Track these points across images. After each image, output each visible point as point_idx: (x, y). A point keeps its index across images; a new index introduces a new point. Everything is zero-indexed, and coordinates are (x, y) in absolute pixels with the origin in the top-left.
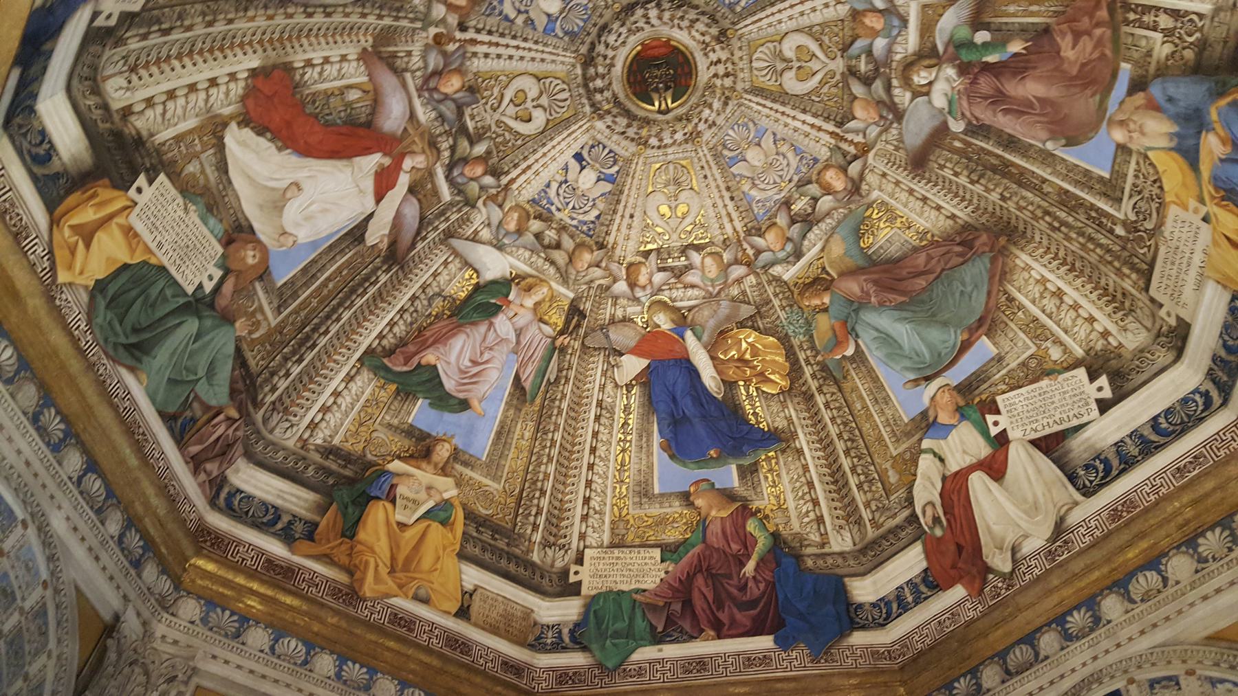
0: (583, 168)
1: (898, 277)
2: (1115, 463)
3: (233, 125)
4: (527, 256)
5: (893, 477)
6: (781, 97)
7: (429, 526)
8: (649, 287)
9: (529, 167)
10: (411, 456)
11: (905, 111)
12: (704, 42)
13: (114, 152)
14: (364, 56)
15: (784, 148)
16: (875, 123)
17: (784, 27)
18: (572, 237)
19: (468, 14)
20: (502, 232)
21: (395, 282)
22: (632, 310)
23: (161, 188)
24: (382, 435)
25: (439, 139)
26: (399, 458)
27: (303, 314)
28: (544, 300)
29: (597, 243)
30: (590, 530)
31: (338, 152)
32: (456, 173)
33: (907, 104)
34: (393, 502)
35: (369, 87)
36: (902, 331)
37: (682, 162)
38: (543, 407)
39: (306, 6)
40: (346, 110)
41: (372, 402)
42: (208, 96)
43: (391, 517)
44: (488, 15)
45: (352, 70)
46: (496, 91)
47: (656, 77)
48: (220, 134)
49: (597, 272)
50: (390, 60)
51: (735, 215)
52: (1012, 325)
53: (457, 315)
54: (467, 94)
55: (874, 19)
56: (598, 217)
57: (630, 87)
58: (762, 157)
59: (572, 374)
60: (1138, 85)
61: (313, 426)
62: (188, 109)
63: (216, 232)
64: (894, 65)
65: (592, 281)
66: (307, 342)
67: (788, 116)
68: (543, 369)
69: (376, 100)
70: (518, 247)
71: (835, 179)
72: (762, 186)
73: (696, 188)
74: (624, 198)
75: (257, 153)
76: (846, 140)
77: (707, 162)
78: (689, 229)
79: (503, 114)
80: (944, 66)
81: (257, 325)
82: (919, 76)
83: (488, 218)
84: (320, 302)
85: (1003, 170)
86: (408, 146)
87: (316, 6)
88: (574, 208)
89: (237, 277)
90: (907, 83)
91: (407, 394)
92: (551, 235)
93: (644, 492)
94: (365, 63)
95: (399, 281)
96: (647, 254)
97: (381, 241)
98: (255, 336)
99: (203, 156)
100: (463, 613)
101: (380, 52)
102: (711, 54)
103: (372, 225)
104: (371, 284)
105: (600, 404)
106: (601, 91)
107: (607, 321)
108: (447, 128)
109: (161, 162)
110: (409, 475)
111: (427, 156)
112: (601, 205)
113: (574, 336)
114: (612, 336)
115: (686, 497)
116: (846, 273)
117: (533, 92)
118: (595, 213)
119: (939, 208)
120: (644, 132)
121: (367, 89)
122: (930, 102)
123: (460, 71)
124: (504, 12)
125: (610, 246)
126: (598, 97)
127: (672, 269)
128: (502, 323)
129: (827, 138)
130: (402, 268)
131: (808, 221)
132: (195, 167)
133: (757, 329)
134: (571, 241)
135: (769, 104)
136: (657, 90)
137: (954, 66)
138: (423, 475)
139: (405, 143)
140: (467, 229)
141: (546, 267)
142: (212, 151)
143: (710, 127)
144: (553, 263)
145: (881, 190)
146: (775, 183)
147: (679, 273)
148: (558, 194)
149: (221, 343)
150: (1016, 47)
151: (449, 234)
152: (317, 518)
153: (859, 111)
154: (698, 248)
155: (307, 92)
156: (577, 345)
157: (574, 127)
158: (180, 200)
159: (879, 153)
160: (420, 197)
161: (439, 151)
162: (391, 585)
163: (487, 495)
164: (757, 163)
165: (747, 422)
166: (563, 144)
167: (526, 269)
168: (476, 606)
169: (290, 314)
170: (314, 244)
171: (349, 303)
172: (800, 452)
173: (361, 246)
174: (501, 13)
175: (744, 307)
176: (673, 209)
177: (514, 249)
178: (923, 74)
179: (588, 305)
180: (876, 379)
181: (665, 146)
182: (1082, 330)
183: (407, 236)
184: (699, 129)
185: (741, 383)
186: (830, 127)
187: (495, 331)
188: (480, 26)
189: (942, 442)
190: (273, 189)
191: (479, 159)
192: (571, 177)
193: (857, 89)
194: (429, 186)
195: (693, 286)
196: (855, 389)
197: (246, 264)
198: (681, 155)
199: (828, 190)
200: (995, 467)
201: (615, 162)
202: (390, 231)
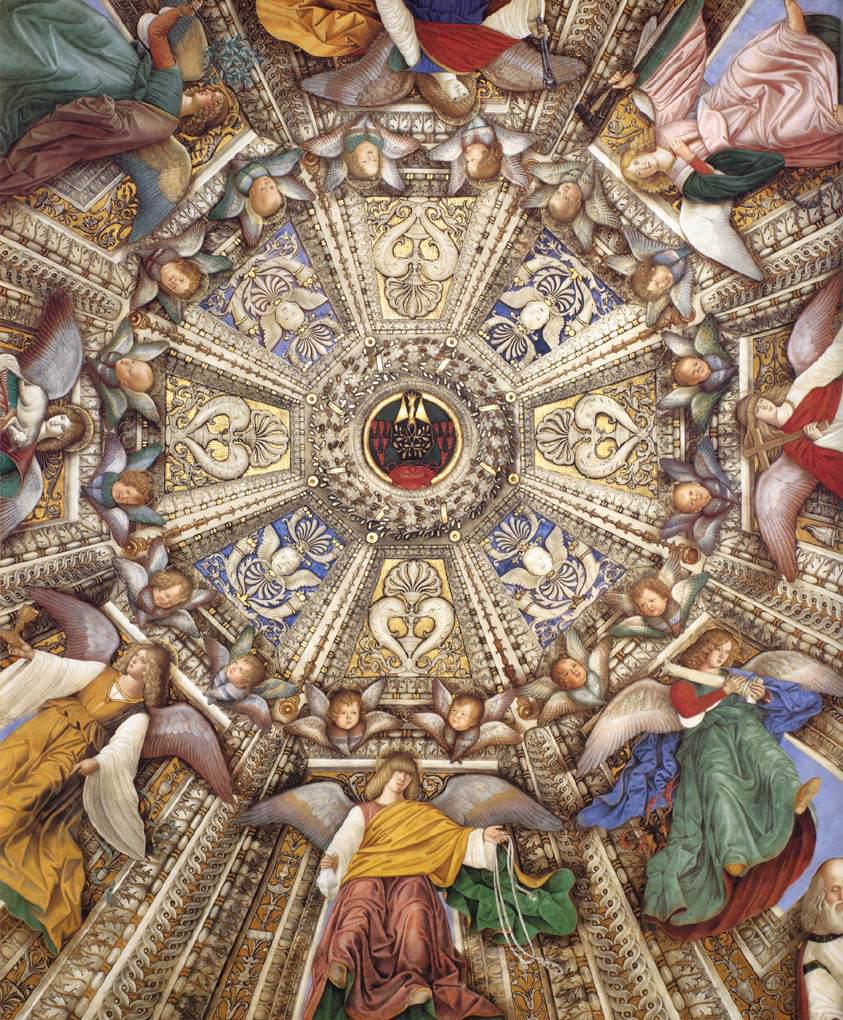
0: (539, 332)
1: (79, 141)
4: (649, 225)
8: (468, 140)
9: (615, 350)
11: (80, 376)
12: (349, 473)
14: (796, 573)
15: (249, 324)
16: (121, 356)
18: (574, 237)
19: (645, 576)
20: (677, 269)
25: (729, 430)
28: (638, 153)
29: (539, 219)
33: (78, 387)
37: (397, 317)
44: (621, 566)
45: (816, 563)
47: (417, 442)
49: (546, 175)
50: (763, 555)
51: (326, 233)
53: (783, 167)
54: (674, 475)
55: (126, 495)
56: (530, 257)
57: (454, 430)
58: (280, 314)
59: (618, 20)
64: (97, 440)
65: (556, 163)
67: (242, 368)
68: (664, 43)
69: (798, 512)
70: (659, 241)
72: (282, 273)
73: (379, 276)
74: (487, 277)
76: (161, 331)
77: (360, 313)
78: (396, 220)
79: (633, 434)
80: (29, 442)
82: (63, 427)
83: (693, 293)
86: (776, 436)
87: (832, 666)
88: (563, 279)
90: (79, 419)
92: (605, 248)
94: (796, 565)
102: (341, 456)
107: (543, 96)
108: (715, 440)
111: (753, 413)
113: (602, 82)
114: (538, 72)
117: (585, 451)
118: (533, 265)
120: (444, 364)
122: (46, 392)
123: (677, 508)
124: (599, 564)
125: (520, 211)
126: (499, 424)
128: (714, 133)
129: (189, 335)
131: (216, 221)
134: (577, 232)
137: (16, 443)
139: (778, 443)
140: (729, 287)
141: (624, 202)
143: (352, 360)
144: (611, 205)
146: (264, 278)
147: (419, 155)
148: (582, 302)
151: (759, 287)
153: (144, 371)
157: (540, 389)
159: (115, 314)
160: (781, 359)
161: (736, 414)
164: (289, 306)
166: (560, 370)
167: (652, 206)
174: (603, 565)
177: (666, 241)
178: (57, 430)
179: (570, 126)
181: (416, 342)
184: (367, 359)
186: (183, 349)
187: (728, 127)
188: (633, 555)
192: (558, 324)
193: (146, 403)
198: (397, 326)
199: (187, 264)
201: (491, 332)
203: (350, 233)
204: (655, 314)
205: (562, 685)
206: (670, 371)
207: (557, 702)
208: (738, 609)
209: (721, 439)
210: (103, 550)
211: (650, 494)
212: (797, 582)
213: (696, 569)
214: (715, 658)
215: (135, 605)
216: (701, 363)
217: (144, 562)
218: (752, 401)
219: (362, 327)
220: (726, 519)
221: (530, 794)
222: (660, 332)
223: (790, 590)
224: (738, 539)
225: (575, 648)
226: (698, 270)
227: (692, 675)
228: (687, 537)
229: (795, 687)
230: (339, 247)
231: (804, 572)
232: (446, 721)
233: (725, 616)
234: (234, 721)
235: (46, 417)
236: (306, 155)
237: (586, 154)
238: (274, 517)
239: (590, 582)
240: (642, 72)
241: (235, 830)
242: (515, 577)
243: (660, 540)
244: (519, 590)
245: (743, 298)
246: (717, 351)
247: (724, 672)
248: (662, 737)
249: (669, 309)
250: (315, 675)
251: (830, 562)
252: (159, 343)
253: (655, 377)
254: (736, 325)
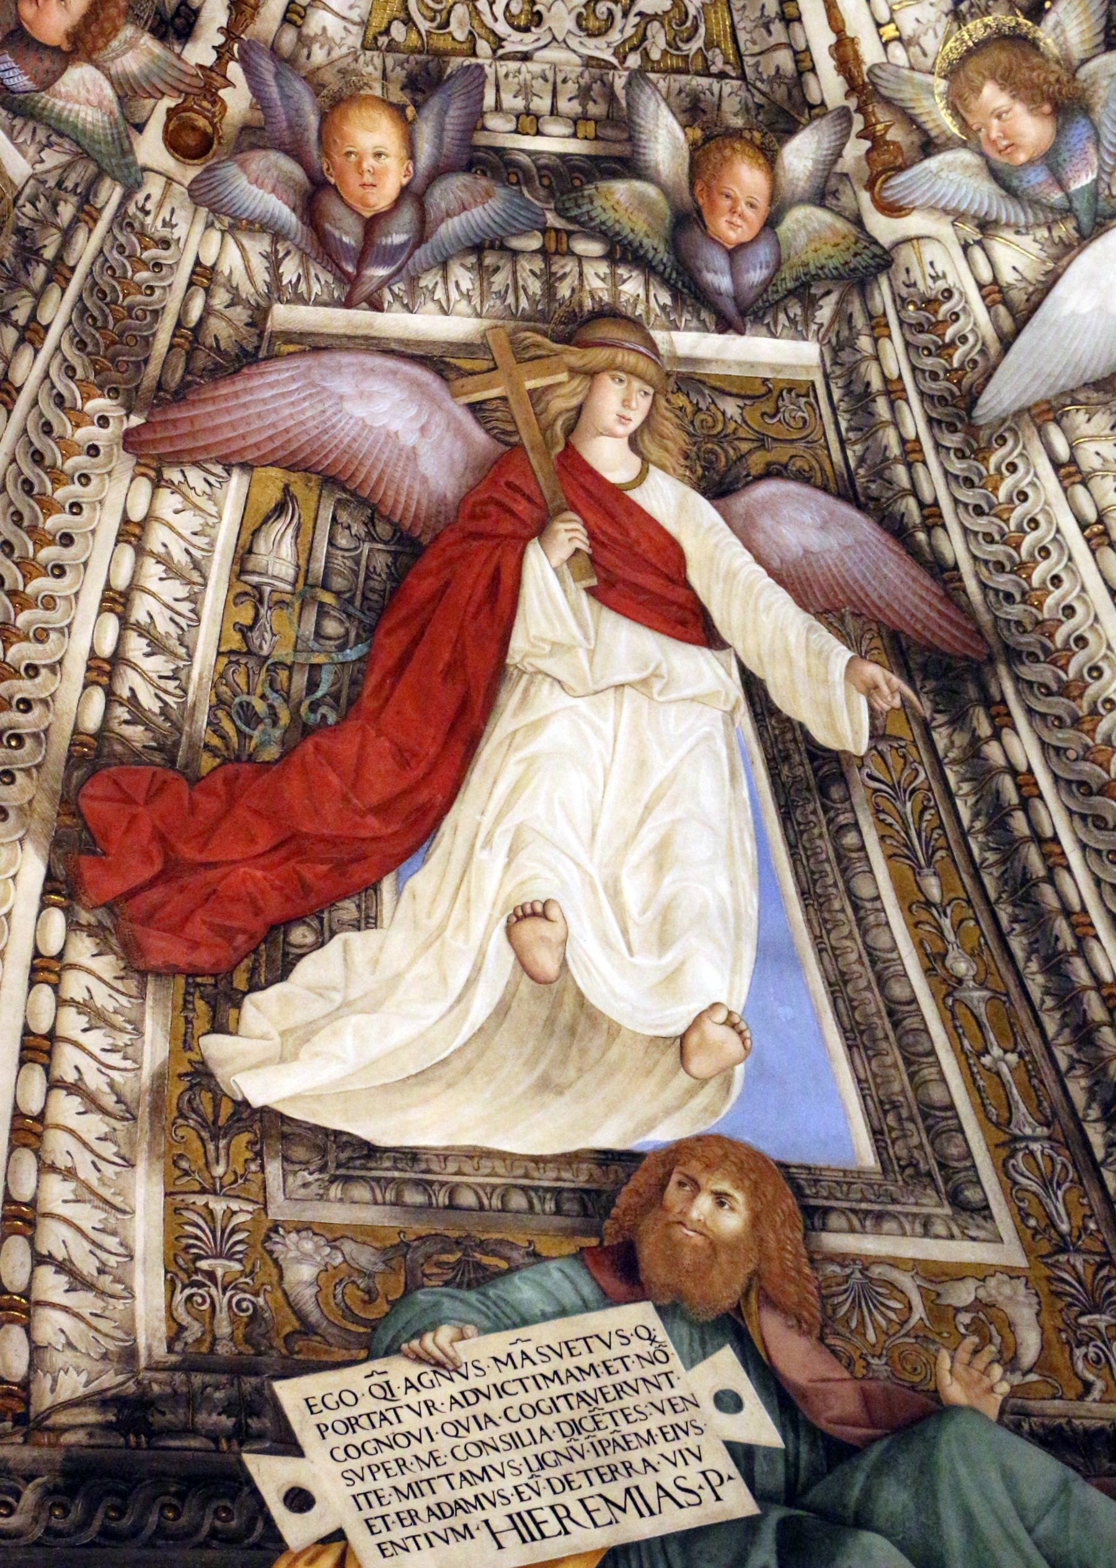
3: (214, 1046)
13: (126, 1522)
20: (1036, 179)
21: (1058, 706)
23: (327, 1417)
25: (564, 290)
27: (1025, 1123)
31: (464, 706)
32: (721, 281)
35: (273, 480)
40: (323, 612)
42: (75, 1089)
45: (188, 522)
48: (226, 1109)
50: (201, 360)
62: (94, 1182)
63: (569, 1297)
75: (346, 1007)
83: (958, 216)
84: (1012, 1039)
86: (546, 429)
89: (770, 1302)
94: (177, 459)
95: (1064, 690)
97: (871, 690)
99: (280, 1209)
101: (160, 386)
104: (1024, 805)
108: (534, 243)
109: (237, 1369)
111: (611, 367)
121: (272, 495)
130: (1014, 656)
132: (304, 1257)
139: (528, 435)
142: (274, 1168)
149: (997, 1487)
155: (202, 719)
158: (398, 1370)
160: (757, 462)
161: (609, 313)
169: (1003, 1169)
171: (1061, 926)
173: (857, 777)
190: (502, 1010)
194: (730, 407)
197: (733, 1246)
202: (844, 637)
204: (905, 94)
206: (738, 122)
208: (40, 272)
209: (538, 265)
211: (378, 23)
212: (125, 463)
216: (755, 218)
218: (643, 365)
220: (305, 257)
222: (852, 103)
223: (101, 436)
224: (246, 290)
226: (1026, 241)
228: (246, 128)
231: (158, 483)
233: (20, 232)
245: (928, 363)
246: (786, 273)
249: (915, 138)
251: (196, 566)
253: (722, 76)
254: (854, 335)
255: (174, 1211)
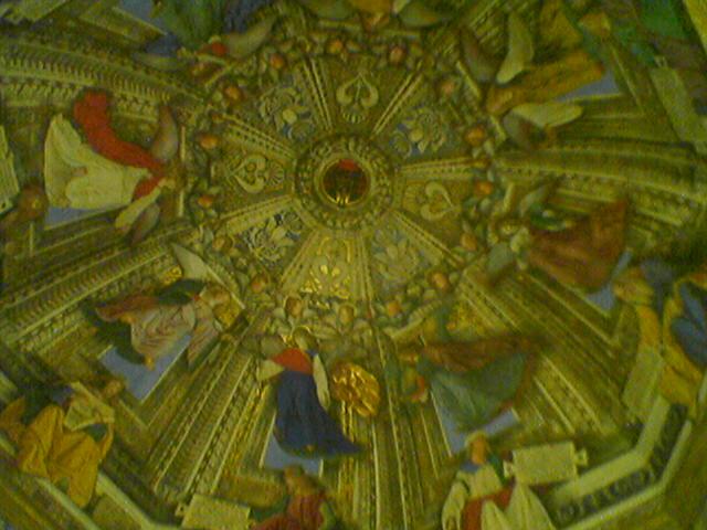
2: (582, 509)
5: (432, 495)
6: (418, 219)
7: (85, 438)
10: (90, 383)
14: (160, 107)
15: (412, 251)
17: (430, 177)
18: (257, 268)
22: (282, 330)
24: (75, 360)
26: (81, 381)
28: (222, 305)
30: (202, 482)
34: (66, 410)
36: (461, 392)
38: (196, 380)
39: (136, 62)
41: (77, 336)
43: (60, 423)
46: (237, 157)
49: (265, 297)
52: (532, 404)
60: (635, 262)
61: (29, 337)
65: (261, 302)
66: (46, 276)
69: (158, 135)
71: (441, 284)
79: (237, 174)
81: (20, 250)
85: (545, 301)
90: (497, 229)
91: (103, 339)
92: (244, 262)
93: (251, 463)
96: (303, 295)
98: (16, 257)
100: (89, 510)
103: (124, 212)
105: (239, 389)
106: (305, 181)
110: (84, 396)
112: (283, 252)
114: (263, 344)
115: (281, 476)
116: (432, 344)
118: (278, 256)
119: (500, 316)
120: (325, 216)
122: (509, 247)
123: (219, 138)
126: (302, 184)
127: (318, 310)
128: (188, 312)
131: (416, 302)
133: (364, 367)
135: (409, 221)
136: (341, 191)
138: (94, 400)
144: (238, 281)
145: (467, 295)
147: (321, 314)
150: (567, 224)
151: (172, 239)
152: (7, 401)
153: (464, 241)
154: (340, 301)
156: (236, 343)
158: (6, 148)
162: (43, 469)
163: (134, 430)
165: (340, 432)
168: (100, 509)
170: (80, 212)
172: (372, 464)
175: (360, 350)
176: (330, 271)
179: (253, 318)
180: (436, 424)
182: (576, 417)
183: (144, 230)
185: (344, 403)
186: (444, 247)
189: (472, 478)
191: (211, 197)
193: (466, 227)
195: (329, 325)
196: (421, 427)
199: (433, 285)
200: (502, 500)
203: (359, 284)
205: (283, 57)
207: (286, 48)
210: (502, 164)
213: (209, 107)
214: (201, 67)
215: (492, 134)
217: (484, 152)
219: (361, 240)
221: (304, 8)
225: (274, 74)
227: (213, 59)
229: (162, 55)
230: (365, 278)
232: (344, 45)
234: (455, 63)
235: (512, 235)
236: (371, 323)
237: (247, 305)
238: (418, 159)
239: (264, 105)
240: (217, 340)
241: (463, 12)
242: (302, 110)
243: (226, 122)
244: (301, 102)
247: (197, 61)
248: (233, 30)
250: (409, 77)
252: (455, 252)
255: (32, 108)
